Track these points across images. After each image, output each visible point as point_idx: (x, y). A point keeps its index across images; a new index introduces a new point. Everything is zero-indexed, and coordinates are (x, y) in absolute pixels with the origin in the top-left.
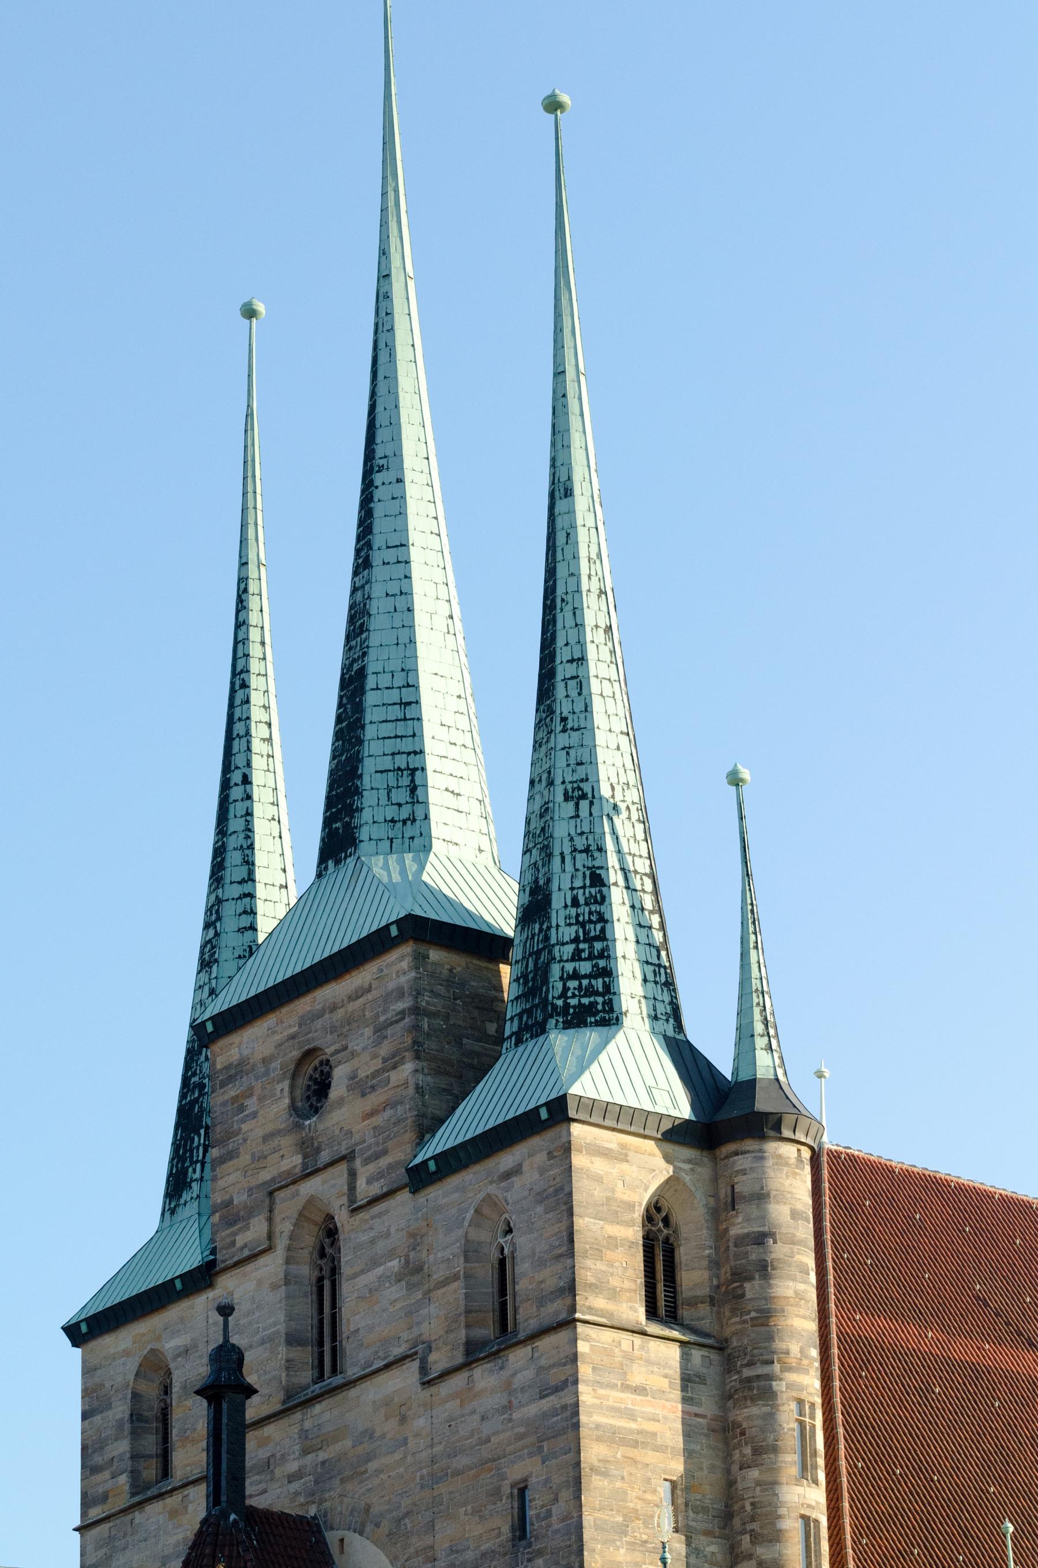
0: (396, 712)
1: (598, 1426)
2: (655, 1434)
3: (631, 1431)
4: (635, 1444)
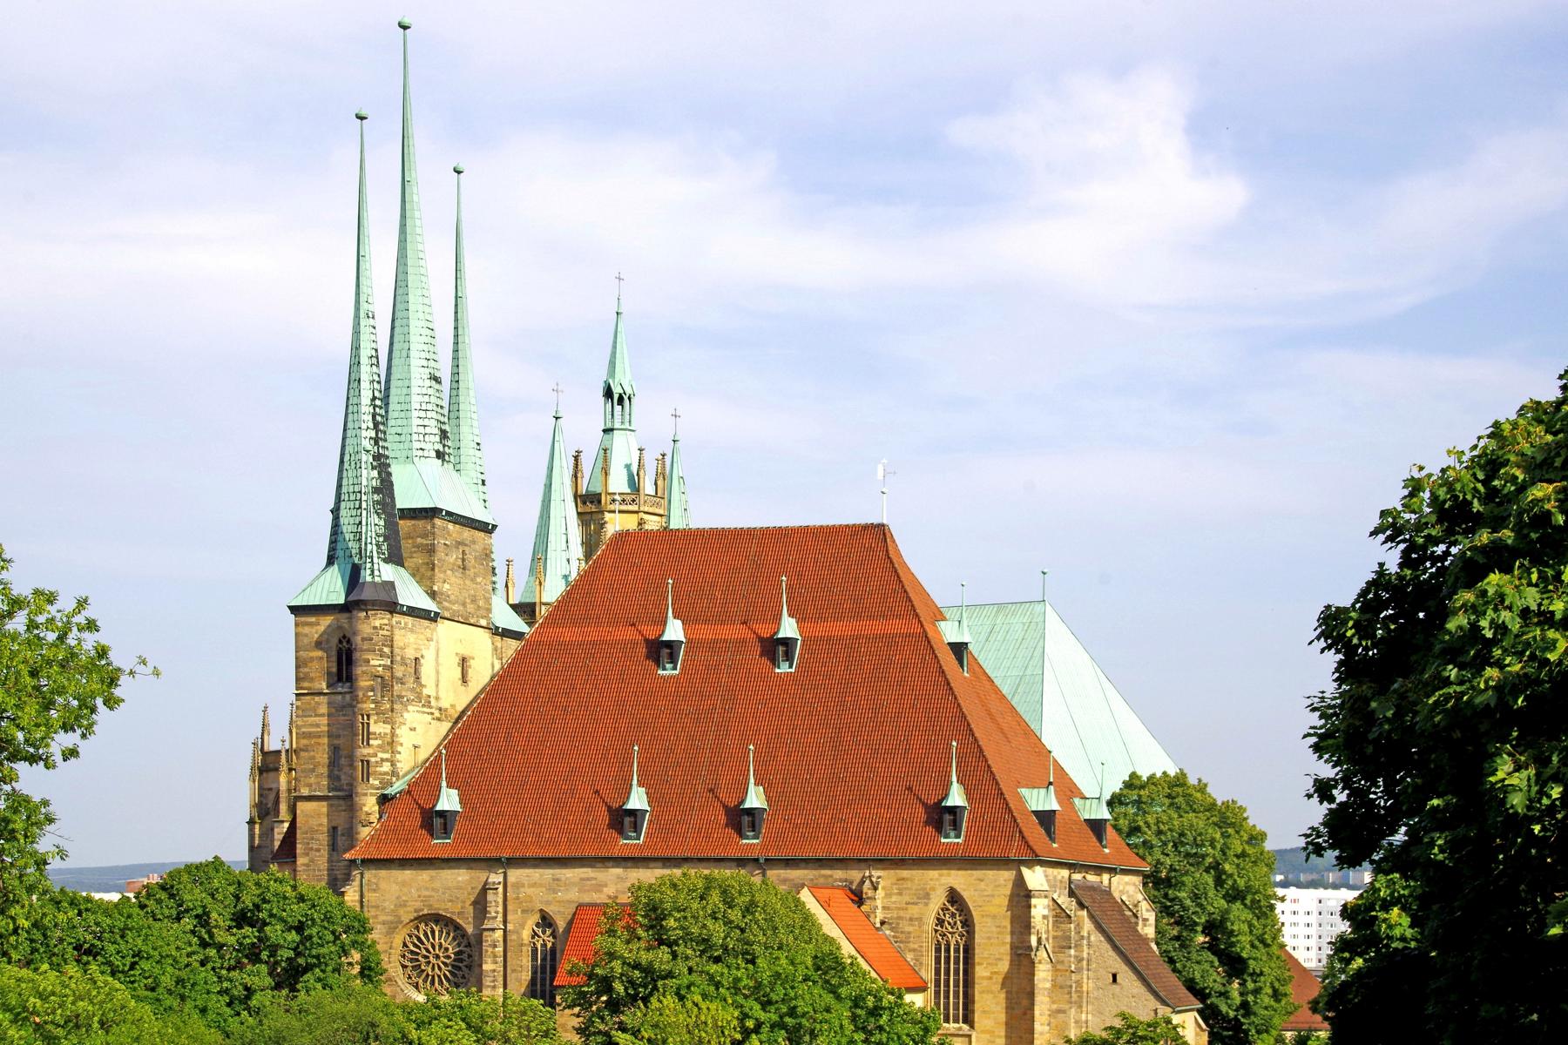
0: (405, 391)
1: (304, 733)
3: (318, 732)
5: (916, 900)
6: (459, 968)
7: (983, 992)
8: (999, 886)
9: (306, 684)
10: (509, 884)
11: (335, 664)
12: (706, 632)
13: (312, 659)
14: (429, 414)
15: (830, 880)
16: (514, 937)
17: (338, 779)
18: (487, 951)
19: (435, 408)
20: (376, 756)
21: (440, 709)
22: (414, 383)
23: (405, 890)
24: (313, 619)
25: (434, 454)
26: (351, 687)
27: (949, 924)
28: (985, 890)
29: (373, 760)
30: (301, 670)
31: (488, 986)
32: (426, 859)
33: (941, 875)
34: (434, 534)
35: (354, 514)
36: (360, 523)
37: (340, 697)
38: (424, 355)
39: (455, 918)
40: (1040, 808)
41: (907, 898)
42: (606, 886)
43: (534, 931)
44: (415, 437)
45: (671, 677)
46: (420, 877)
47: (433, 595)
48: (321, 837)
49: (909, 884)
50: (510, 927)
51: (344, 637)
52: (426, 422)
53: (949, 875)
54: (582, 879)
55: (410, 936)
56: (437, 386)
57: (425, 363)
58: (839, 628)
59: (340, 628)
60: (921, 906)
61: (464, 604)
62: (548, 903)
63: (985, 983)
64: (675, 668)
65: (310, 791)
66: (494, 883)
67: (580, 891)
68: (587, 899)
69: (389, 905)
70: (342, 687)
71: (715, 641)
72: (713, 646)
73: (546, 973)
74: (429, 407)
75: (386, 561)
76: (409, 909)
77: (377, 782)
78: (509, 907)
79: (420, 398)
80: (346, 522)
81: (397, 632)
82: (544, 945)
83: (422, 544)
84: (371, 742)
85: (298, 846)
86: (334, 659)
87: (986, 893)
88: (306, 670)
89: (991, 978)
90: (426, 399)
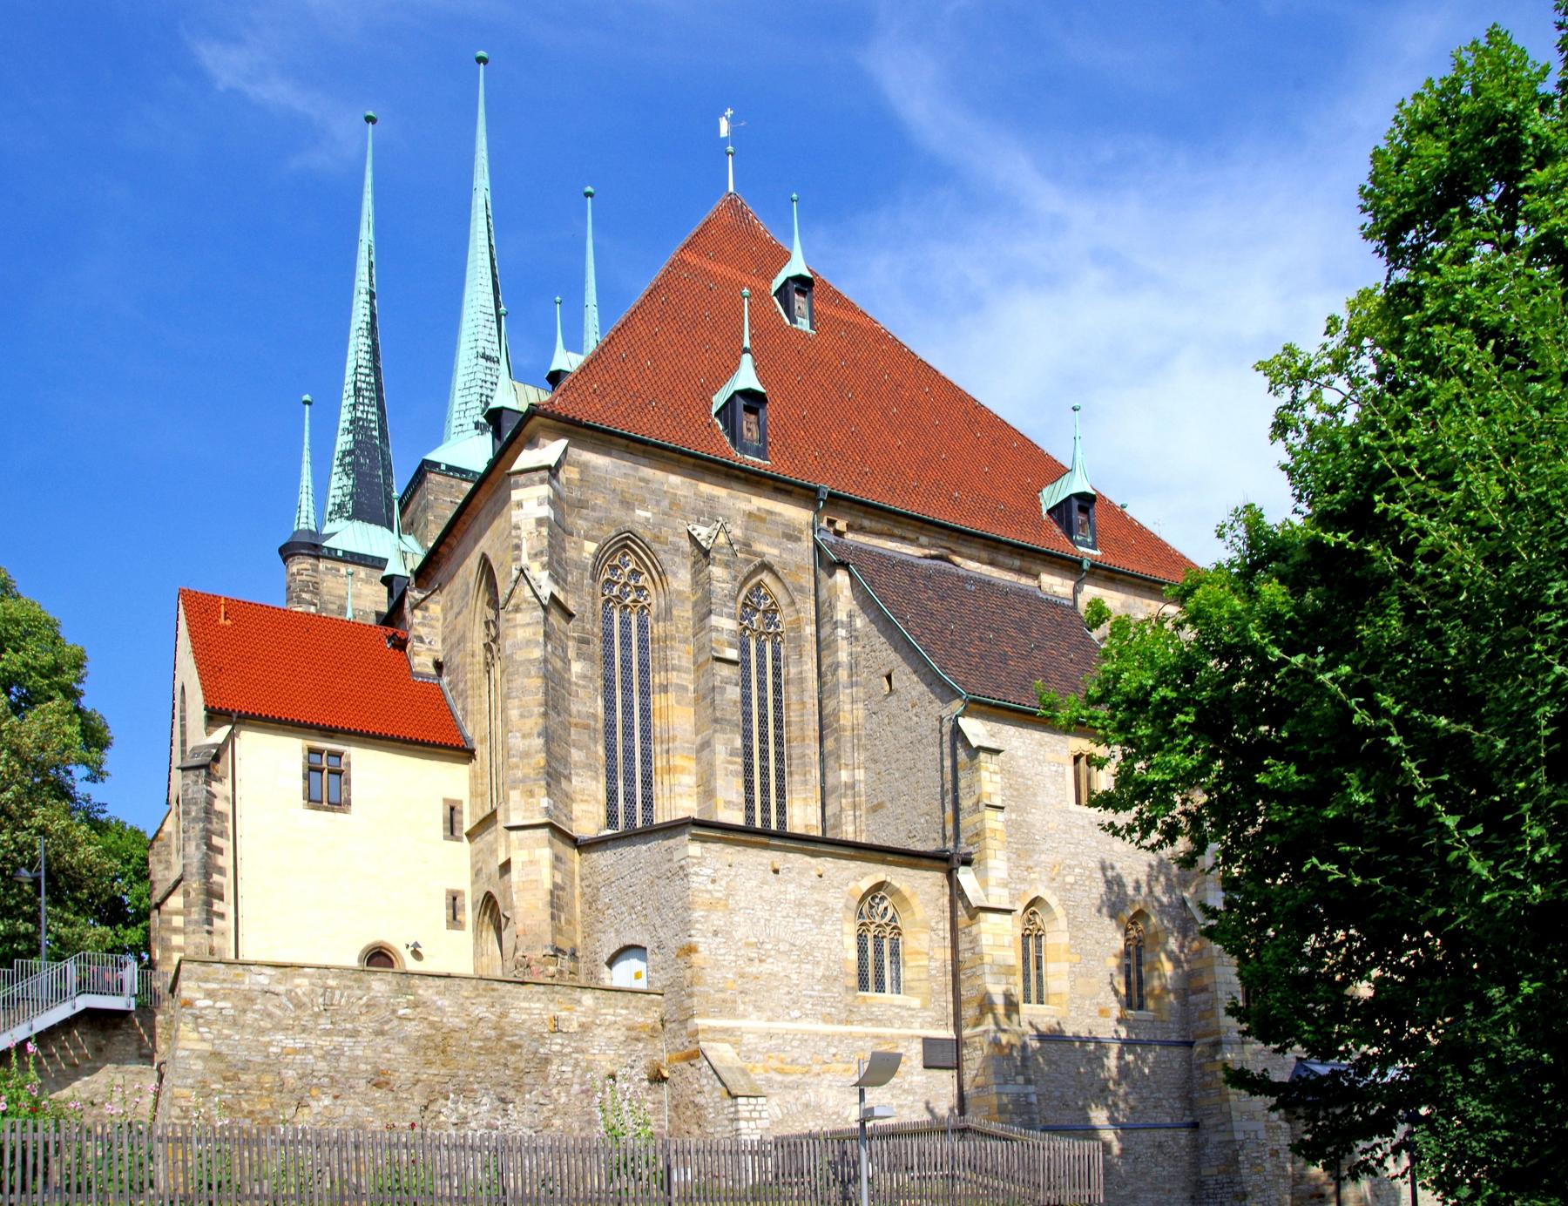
14: (472, 390)
19: (480, 383)
38: (473, 338)
52: (469, 398)
56: (489, 364)
57: (473, 344)
75: (348, 519)
79: (466, 378)
90: (472, 376)
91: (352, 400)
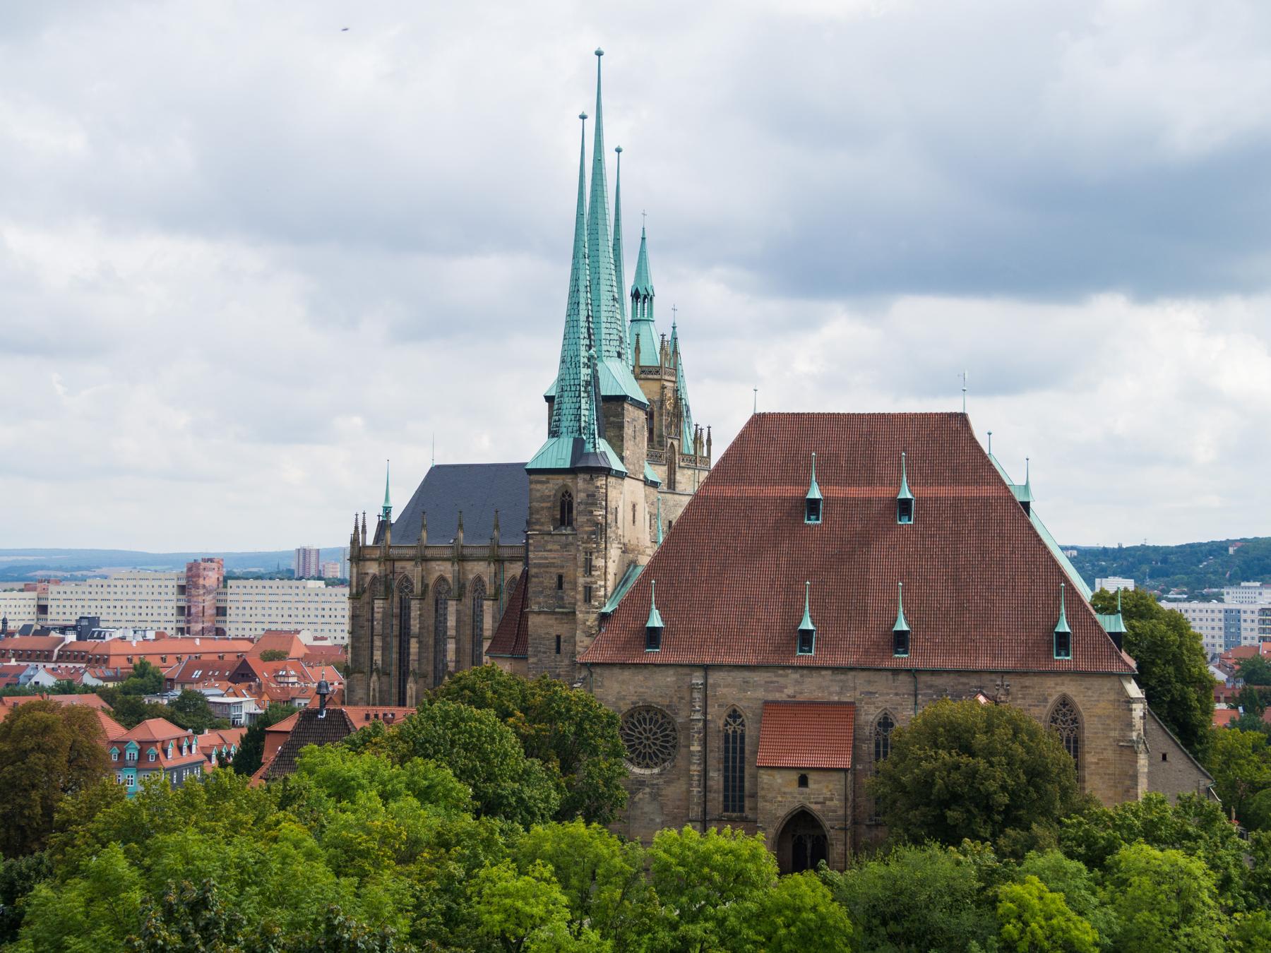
2: (554, 563)
4: (548, 567)
5: (1037, 703)
6: (666, 748)
7: (1092, 774)
8: (1103, 693)
9: (538, 527)
10: (708, 685)
11: (559, 512)
12: (838, 492)
13: (542, 508)
14: (613, 326)
15: (967, 687)
16: (712, 725)
17: (562, 599)
18: (694, 736)
20: (596, 583)
21: (624, 544)
22: (603, 302)
23: (624, 687)
24: (543, 478)
25: (616, 355)
26: (573, 529)
27: (1062, 721)
28: (1092, 696)
29: (594, 586)
30: (534, 516)
31: (695, 763)
32: (642, 664)
33: (1057, 684)
34: (623, 414)
35: (575, 401)
36: (580, 407)
37: (564, 538)
38: (608, 283)
39: (665, 709)
40: (1113, 631)
41: (1029, 701)
42: (786, 688)
43: (726, 720)
44: (603, 342)
45: (816, 526)
46: (636, 678)
47: (622, 459)
48: (547, 643)
49: (1031, 691)
50: (709, 717)
51: (567, 492)
53: (1063, 684)
54: (766, 682)
55: (627, 722)
57: (610, 289)
58: (946, 491)
59: (565, 485)
60: (1041, 708)
61: (634, 465)
62: (740, 700)
63: (1093, 767)
64: (818, 519)
65: (539, 608)
66: (697, 684)
67: (765, 691)
68: (770, 697)
69: (611, 699)
70: (565, 530)
71: (846, 499)
72: (844, 502)
73: (736, 753)
74: (613, 320)
76: (628, 701)
77: (597, 603)
78: (708, 702)
79: (607, 314)
80: (569, 407)
81: (609, 489)
82: (734, 732)
83: (613, 422)
84: (593, 573)
85: (530, 649)
86: (559, 508)
87: (1093, 699)
88: (538, 516)
89: (1098, 764)
90: (611, 314)
91: (588, 343)
